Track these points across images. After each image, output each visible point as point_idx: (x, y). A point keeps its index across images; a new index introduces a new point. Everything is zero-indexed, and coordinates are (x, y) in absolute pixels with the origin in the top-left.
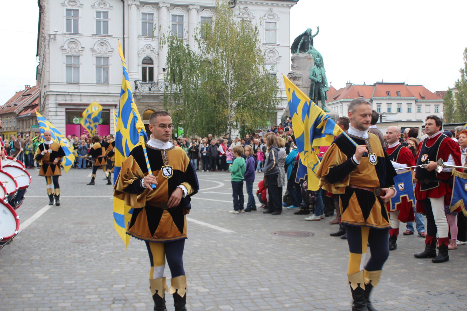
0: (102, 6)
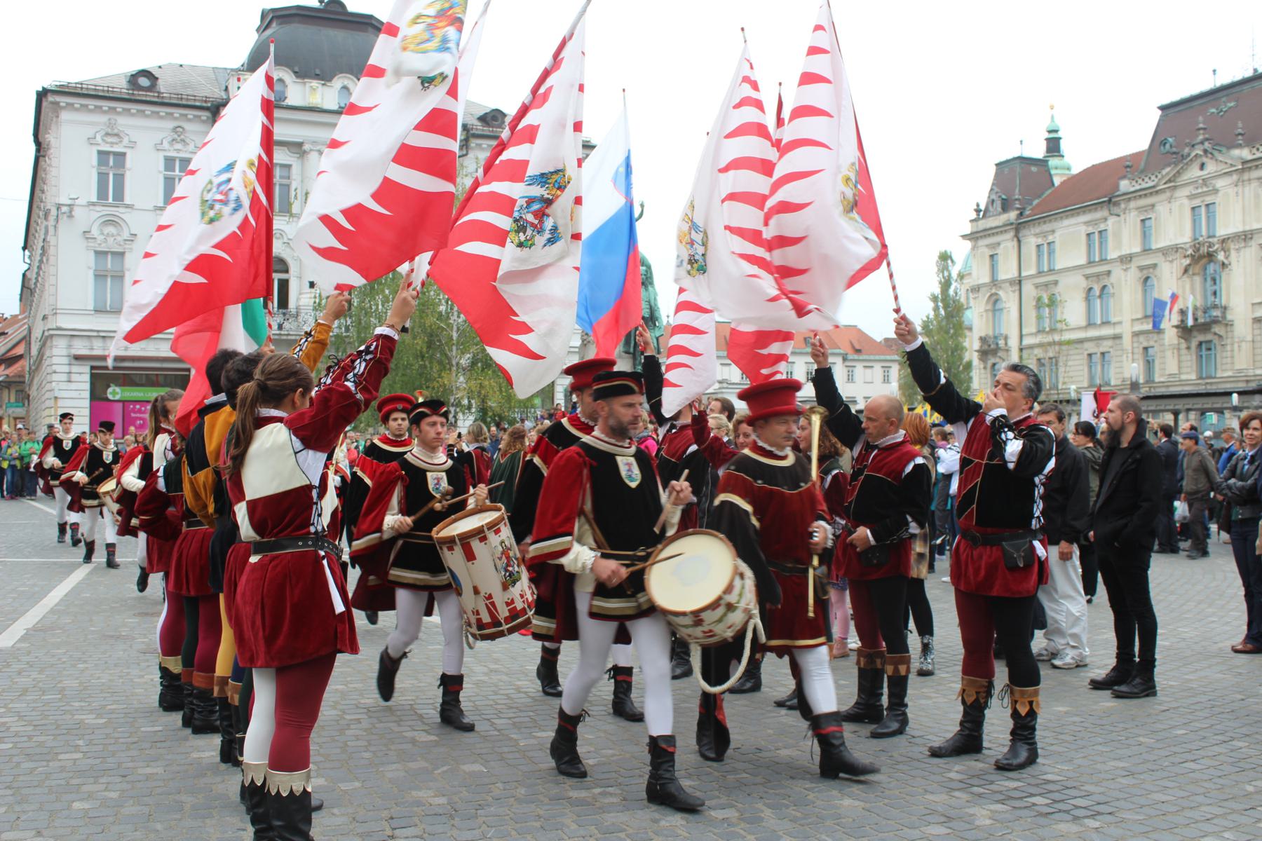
0: (179, 146)
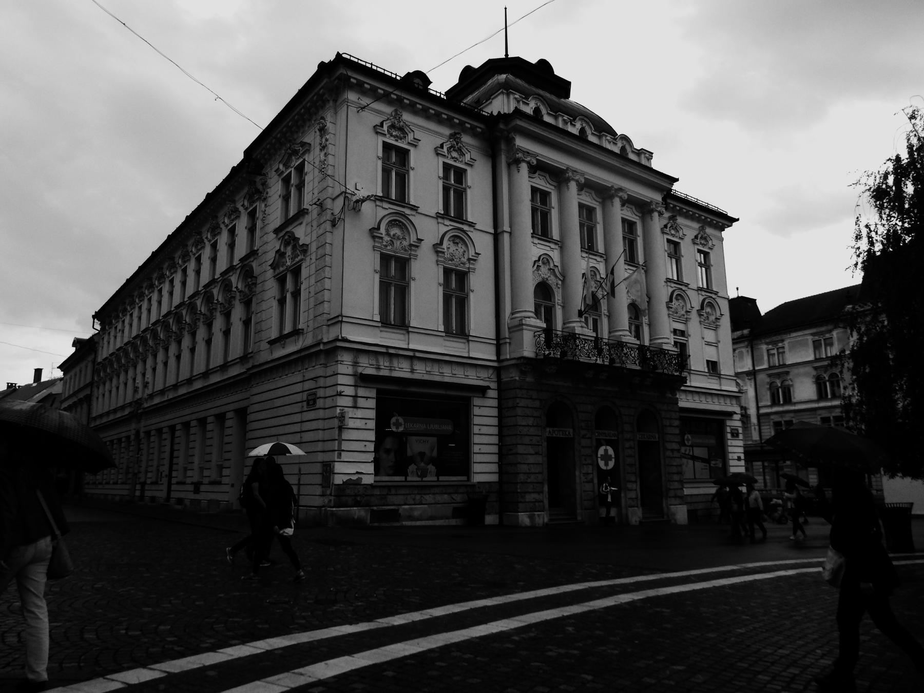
0: (455, 154)
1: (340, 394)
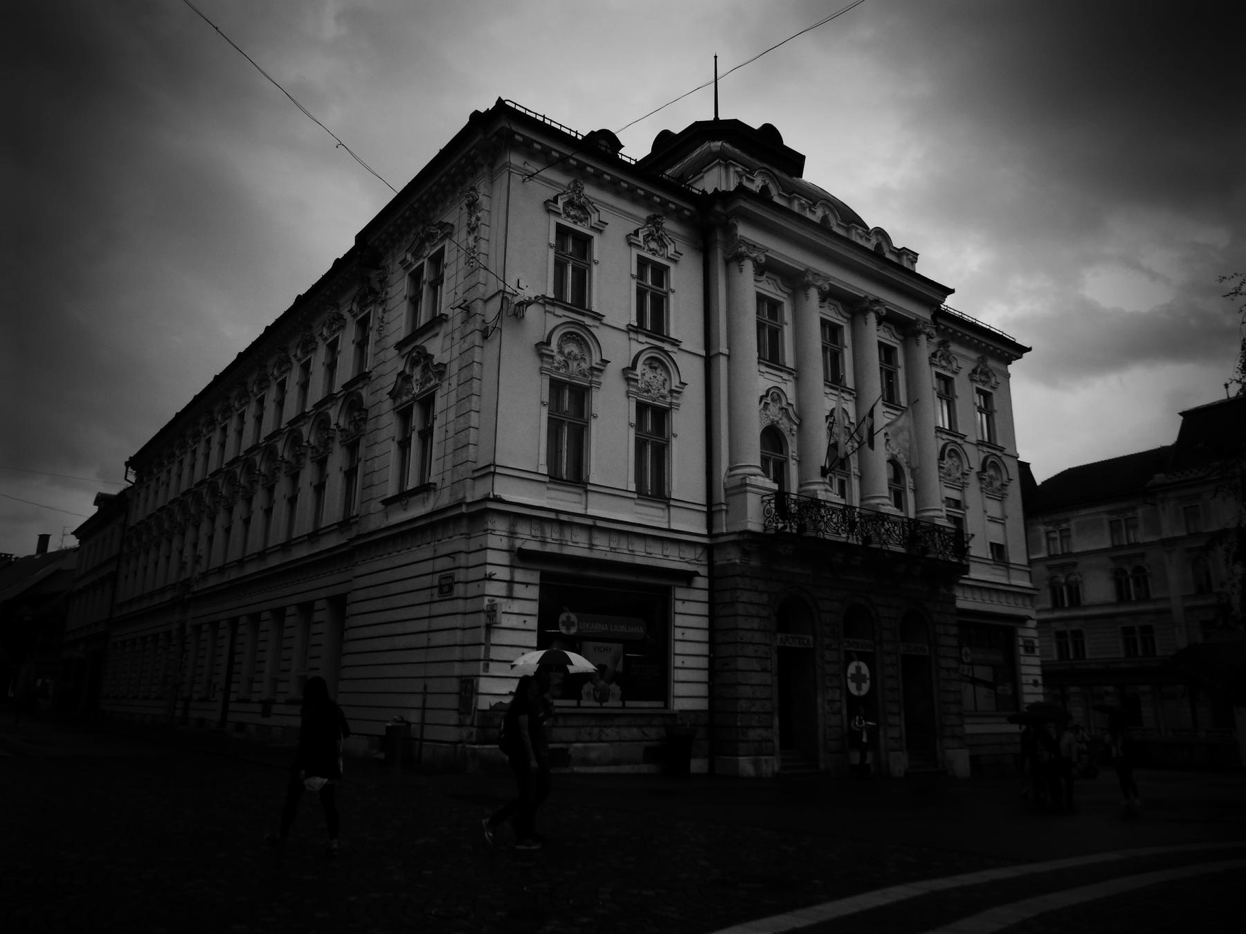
0: (653, 245)
1: (489, 578)
